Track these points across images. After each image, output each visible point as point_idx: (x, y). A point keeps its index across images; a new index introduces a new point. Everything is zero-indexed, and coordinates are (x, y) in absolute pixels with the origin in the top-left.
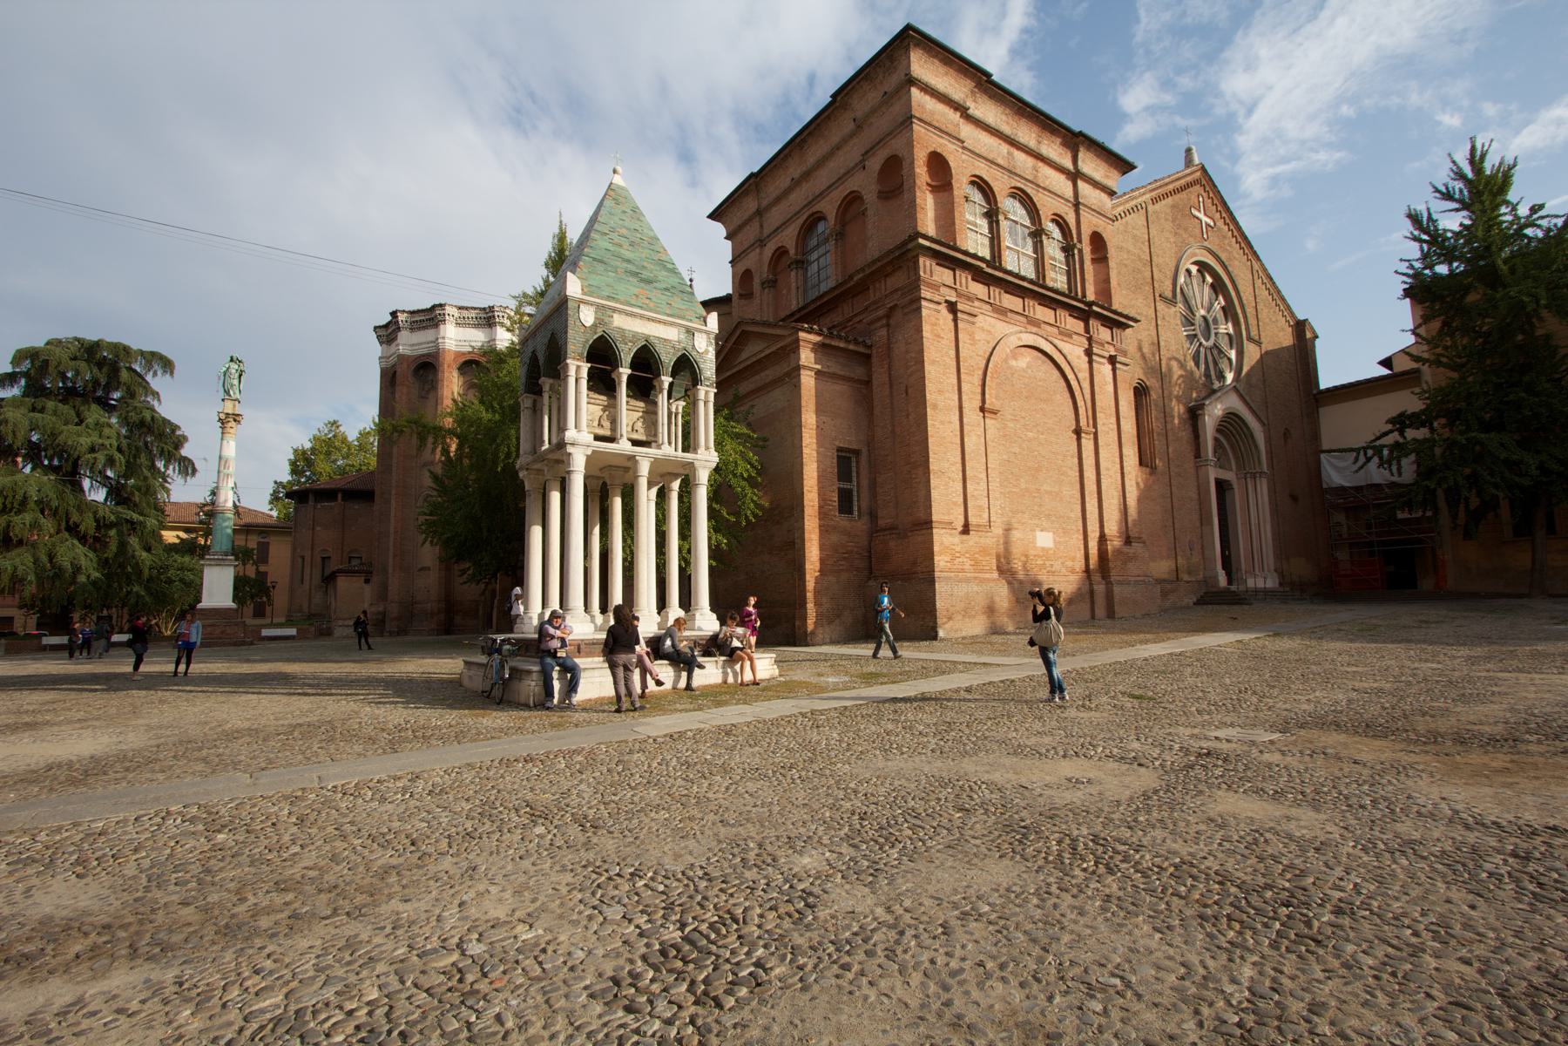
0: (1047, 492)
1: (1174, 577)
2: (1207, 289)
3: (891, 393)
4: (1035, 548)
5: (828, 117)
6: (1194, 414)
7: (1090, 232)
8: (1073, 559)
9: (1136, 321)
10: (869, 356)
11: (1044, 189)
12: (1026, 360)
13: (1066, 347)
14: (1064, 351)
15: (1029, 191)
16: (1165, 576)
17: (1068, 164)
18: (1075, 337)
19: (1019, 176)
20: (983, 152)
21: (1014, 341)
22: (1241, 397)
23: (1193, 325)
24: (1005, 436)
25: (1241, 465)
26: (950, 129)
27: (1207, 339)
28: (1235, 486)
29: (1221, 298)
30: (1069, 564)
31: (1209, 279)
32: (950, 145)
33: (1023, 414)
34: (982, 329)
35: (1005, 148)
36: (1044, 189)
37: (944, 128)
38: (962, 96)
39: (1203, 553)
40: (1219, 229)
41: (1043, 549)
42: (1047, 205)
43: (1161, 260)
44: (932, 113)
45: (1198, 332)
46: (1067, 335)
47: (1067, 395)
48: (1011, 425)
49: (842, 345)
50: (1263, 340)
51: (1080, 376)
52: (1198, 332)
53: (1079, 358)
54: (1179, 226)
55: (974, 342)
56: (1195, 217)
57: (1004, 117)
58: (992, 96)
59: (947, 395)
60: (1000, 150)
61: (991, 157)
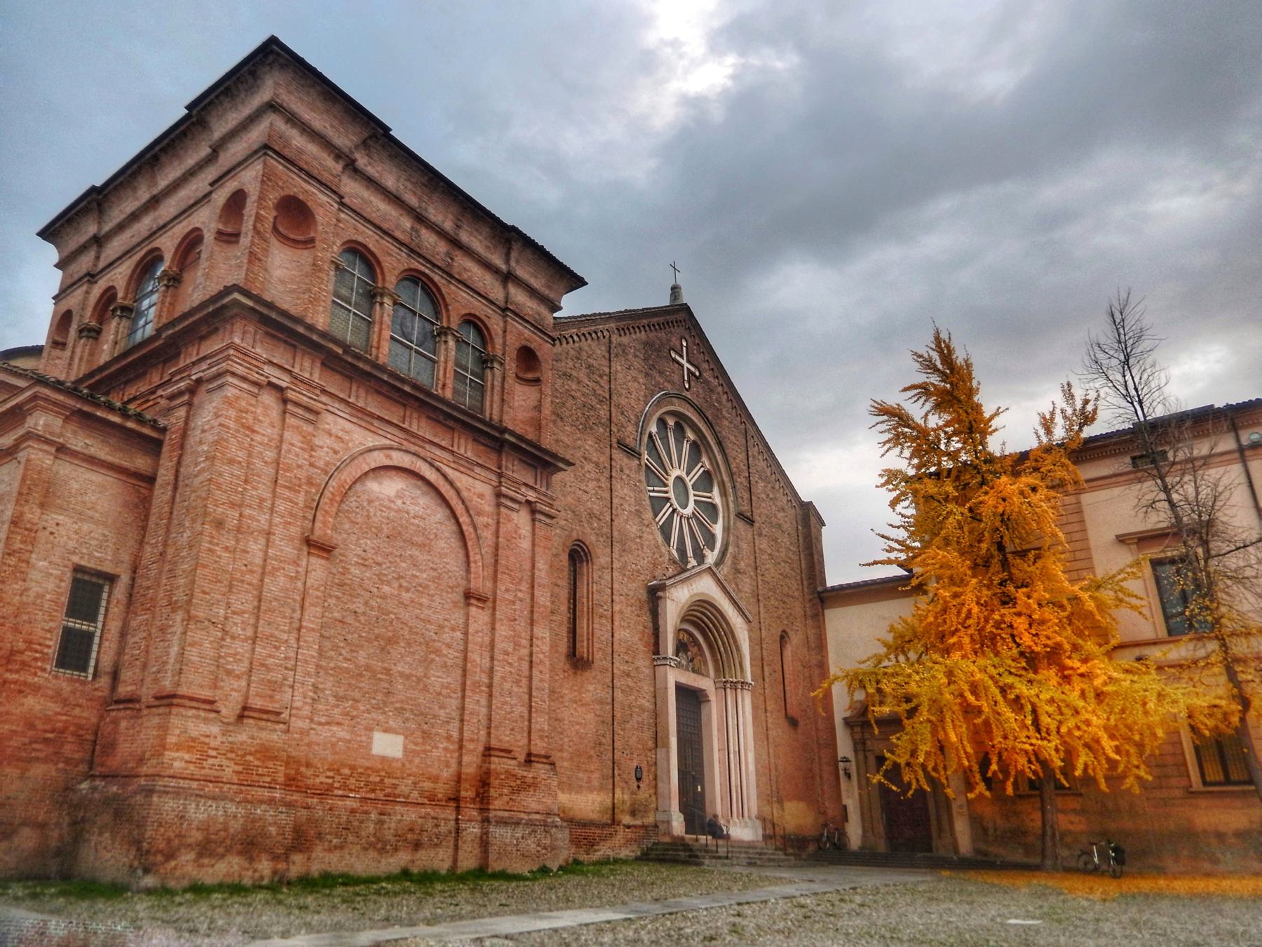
0: (402, 674)
1: (606, 819)
2: (686, 447)
3: (173, 498)
4: (369, 756)
5: (184, 134)
6: (654, 596)
7: (518, 345)
8: (435, 779)
9: (570, 464)
10: (158, 444)
11: (460, 282)
12: (390, 487)
13: (462, 481)
14: (458, 484)
15: (436, 278)
17: (498, 261)
18: (478, 470)
19: (424, 258)
20: (373, 216)
21: (378, 459)
22: (718, 581)
23: (666, 485)
24: (341, 585)
25: (720, 671)
26: (326, 177)
27: (685, 507)
28: (712, 697)
29: (705, 459)
30: (427, 785)
31: (690, 435)
32: (320, 196)
33: (379, 559)
34: (330, 435)
35: (407, 223)
36: (460, 282)
37: (315, 173)
38: (349, 144)
39: (656, 787)
40: (706, 382)
41: (383, 759)
42: (461, 302)
43: (623, 401)
44: (301, 151)
45: (671, 495)
46: (468, 466)
47: (455, 543)
48: (355, 571)
49: (115, 419)
50: (756, 518)
51: (481, 520)
52: (671, 495)
53: (481, 496)
54: (652, 367)
56: (674, 360)
57: (409, 185)
58: (392, 157)
59: (247, 512)
61: (385, 226)
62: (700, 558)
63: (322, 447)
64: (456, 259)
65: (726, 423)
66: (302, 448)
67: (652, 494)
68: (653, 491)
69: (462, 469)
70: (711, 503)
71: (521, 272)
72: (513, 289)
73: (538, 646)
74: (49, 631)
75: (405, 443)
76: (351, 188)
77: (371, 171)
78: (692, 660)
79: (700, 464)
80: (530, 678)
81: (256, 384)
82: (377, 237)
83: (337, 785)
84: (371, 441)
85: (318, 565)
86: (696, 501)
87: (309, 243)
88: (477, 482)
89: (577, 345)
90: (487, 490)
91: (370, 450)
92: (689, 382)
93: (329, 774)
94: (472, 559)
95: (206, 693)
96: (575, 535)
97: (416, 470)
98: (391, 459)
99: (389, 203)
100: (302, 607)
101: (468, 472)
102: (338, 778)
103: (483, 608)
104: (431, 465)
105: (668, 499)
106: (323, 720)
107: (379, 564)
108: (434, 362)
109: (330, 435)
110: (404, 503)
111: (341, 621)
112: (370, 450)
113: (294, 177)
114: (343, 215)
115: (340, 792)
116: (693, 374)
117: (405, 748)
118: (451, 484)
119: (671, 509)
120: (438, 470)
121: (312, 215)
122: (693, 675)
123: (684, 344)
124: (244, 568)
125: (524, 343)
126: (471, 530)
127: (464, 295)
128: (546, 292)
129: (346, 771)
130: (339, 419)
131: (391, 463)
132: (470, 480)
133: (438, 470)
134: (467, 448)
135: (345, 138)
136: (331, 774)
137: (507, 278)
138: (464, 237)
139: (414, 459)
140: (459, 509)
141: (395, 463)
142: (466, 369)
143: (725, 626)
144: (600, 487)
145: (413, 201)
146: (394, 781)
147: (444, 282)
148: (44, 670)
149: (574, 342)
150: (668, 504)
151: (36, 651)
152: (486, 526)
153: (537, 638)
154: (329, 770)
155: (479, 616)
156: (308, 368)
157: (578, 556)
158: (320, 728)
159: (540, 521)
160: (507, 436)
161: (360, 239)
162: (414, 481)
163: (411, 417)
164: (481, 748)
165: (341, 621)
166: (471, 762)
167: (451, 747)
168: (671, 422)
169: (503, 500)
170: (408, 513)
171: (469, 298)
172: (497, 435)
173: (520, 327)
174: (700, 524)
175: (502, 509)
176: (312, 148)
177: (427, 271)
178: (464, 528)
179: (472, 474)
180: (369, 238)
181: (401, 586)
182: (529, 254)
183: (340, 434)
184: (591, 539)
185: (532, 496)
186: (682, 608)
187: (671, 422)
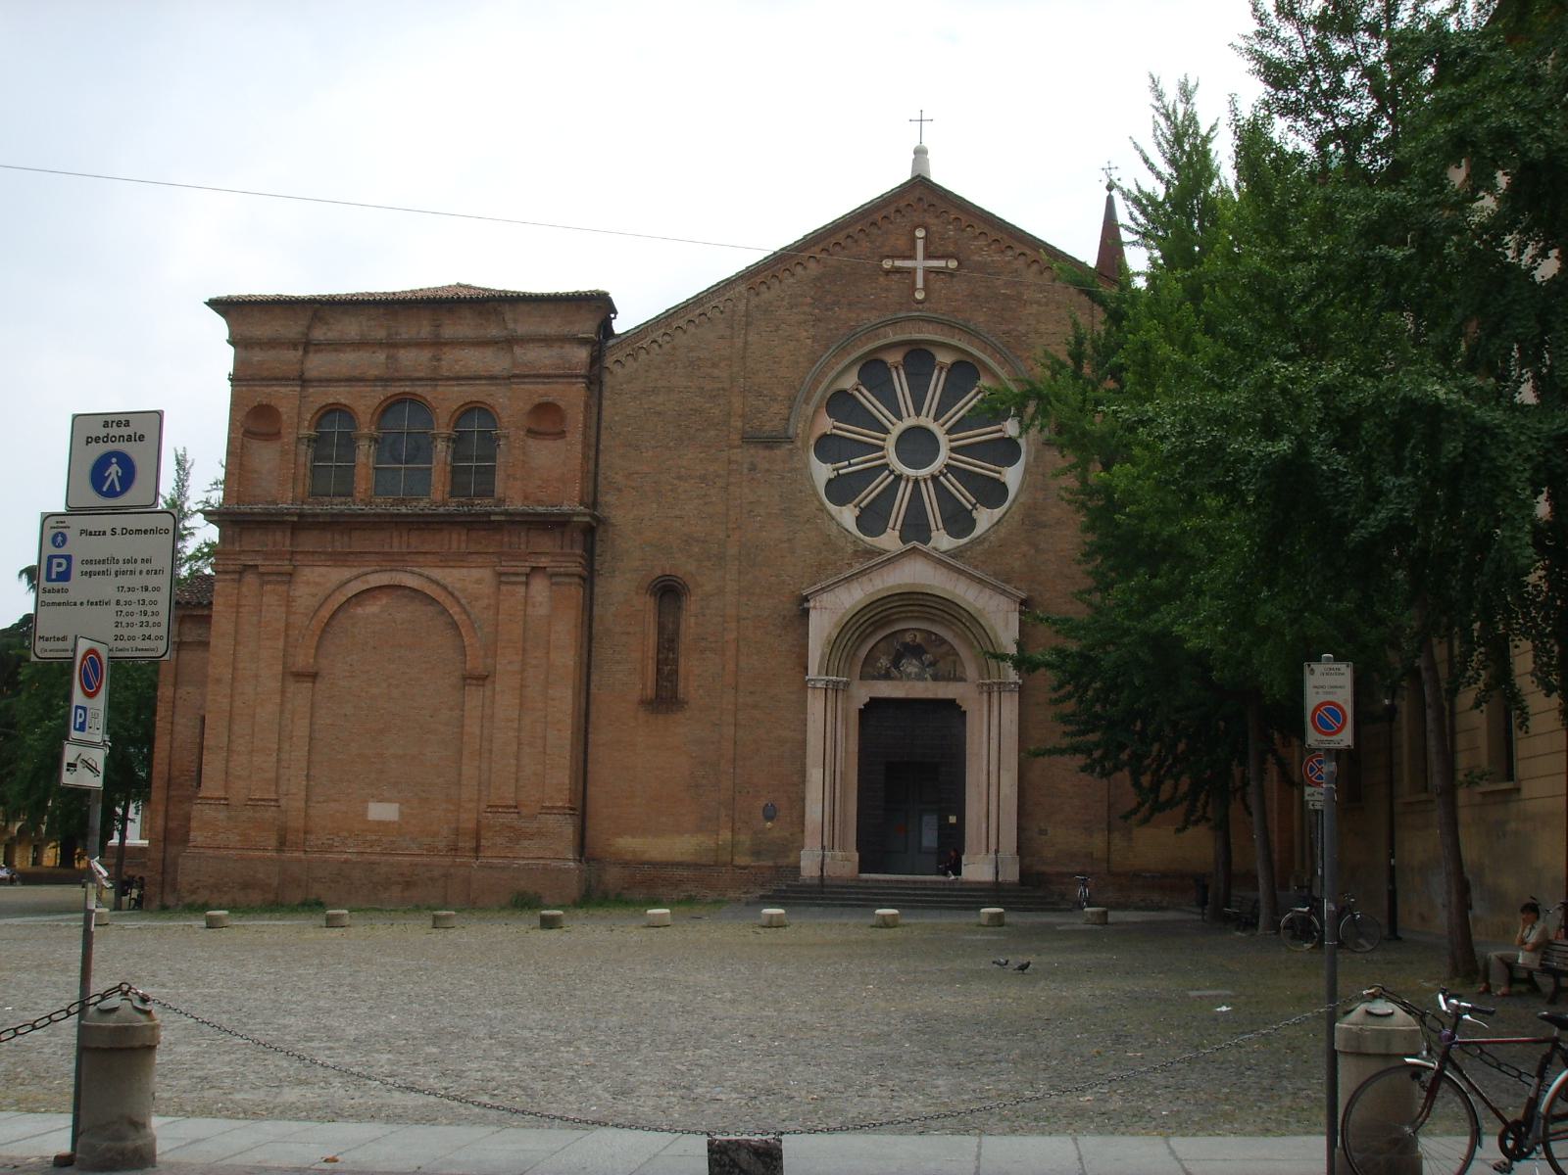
7: (528, 407)
12: (371, 609)
13: (451, 576)
15: (419, 390)
16: (679, 858)
17: (494, 331)
34: (308, 583)
35: (381, 357)
41: (380, 823)
46: (460, 559)
53: (479, 581)
55: (289, 602)
56: (888, 272)
57: (373, 323)
60: (374, 362)
61: (356, 373)
62: (958, 521)
63: (300, 597)
64: (443, 357)
65: (1035, 308)
66: (280, 606)
67: (841, 472)
68: (850, 465)
69: (451, 564)
70: (1003, 438)
71: (522, 329)
72: (517, 350)
73: (555, 707)
74: (192, 762)
75: (384, 563)
76: (318, 364)
77: (331, 335)
78: (932, 664)
79: (977, 389)
80: (545, 738)
81: (234, 572)
82: (347, 389)
83: (335, 844)
84: (346, 573)
85: (300, 692)
86: (953, 450)
87: (276, 435)
88: (473, 570)
89: (666, 347)
90: (486, 574)
91: (350, 581)
92: (926, 288)
93: (328, 837)
94: (466, 644)
95: (222, 794)
96: (658, 572)
97: (396, 583)
98: (368, 582)
99: (359, 350)
100: (292, 721)
101: (461, 564)
102: (336, 839)
103: (483, 685)
104: (413, 573)
105: (886, 466)
106: (321, 799)
107: (368, 672)
108: (430, 469)
109: (308, 583)
110: (390, 614)
111: (332, 725)
112: (350, 581)
113: (257, 388)
114: (311, 390)
115: (339, 849)
116: (938, 272)
117: (401, 813)
118: (437, 583)
119: (892, 477)
120: (421, 575)
121: (278, 411)
122: (930, 684)
123: (920, 233)
124: (242, 705)
125: (537, 400)
126: (464, 617)
127: (456, 388)
128: (566, 330)
129: (347, 835)
130: (316, 568)
131: (368, 587)
132: (465, 571)
133: (421, 575)
134: (457, 541)
135: (292, 329)
136: (331, 837)
137: (510, 342)
138: (448, 331)
139: (394, 574)
140: (447, 602)
141: (373, 585)
142: (469, 458)
143: (965, 614)
144: (706, 504)
145: (381, 334)
146: (391, 839)
147: (429, 388)
148: (192, 786)
149: (660, 346)
150: (887, 472)
151: (186, 775)
152: (488, 607)
153: (553, 700)
154: (329, 834)
155: (474, 698)
156: (281, 540)
157: (668, 592)
158: (319, 805)
159: (556, 584)
160: (493, 518)
161: (331, 401)
162: (399, 592)
163: (391, 537)
164: (483, 806)
165: (332, 725)
166: (468, 821)
167: (452, 808)
168: (893, 358)
169: (503, 579)
170: (395, 622)
171: (464, 388)
172: (485, 519)
173: (531, 387)
174: (964, 476)
175: (504, 588)
176: (271, 354)
177: (407, 389)
178: (456, 618)
179: (466, 564)
180: (340, 395)
181: (389, 685)
182: (523, 307)
183: (317, 579)
184: (684, 566)
185: (543, 561)
186: (844, 615)
187: (893, 358)
